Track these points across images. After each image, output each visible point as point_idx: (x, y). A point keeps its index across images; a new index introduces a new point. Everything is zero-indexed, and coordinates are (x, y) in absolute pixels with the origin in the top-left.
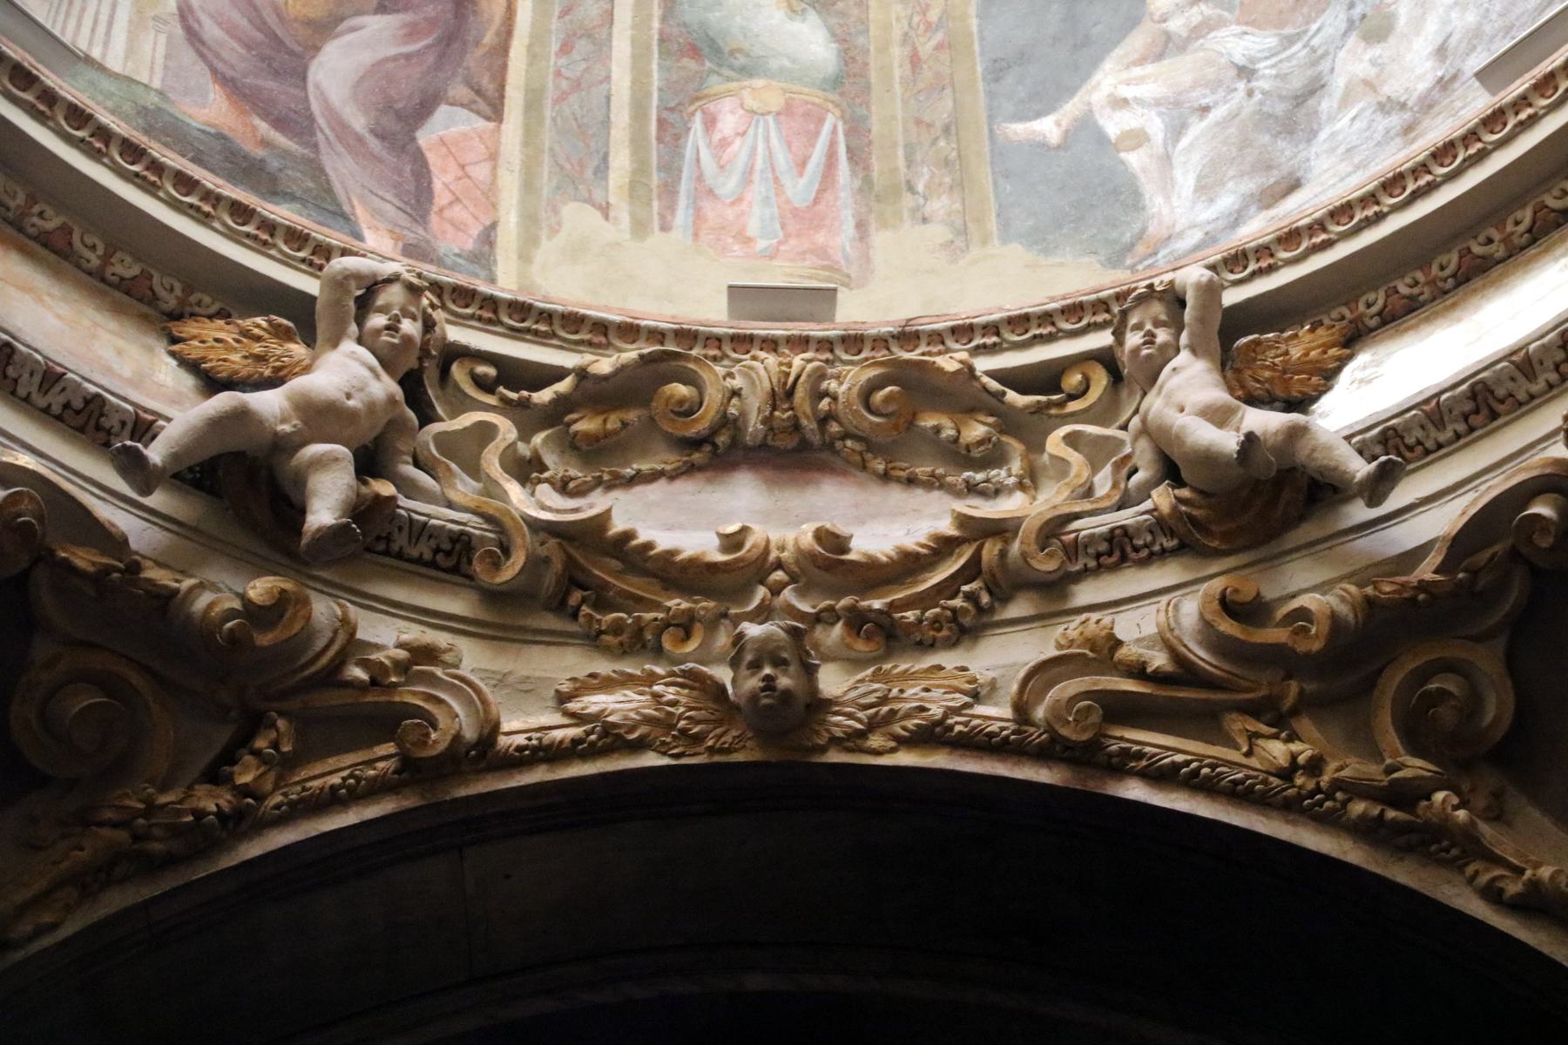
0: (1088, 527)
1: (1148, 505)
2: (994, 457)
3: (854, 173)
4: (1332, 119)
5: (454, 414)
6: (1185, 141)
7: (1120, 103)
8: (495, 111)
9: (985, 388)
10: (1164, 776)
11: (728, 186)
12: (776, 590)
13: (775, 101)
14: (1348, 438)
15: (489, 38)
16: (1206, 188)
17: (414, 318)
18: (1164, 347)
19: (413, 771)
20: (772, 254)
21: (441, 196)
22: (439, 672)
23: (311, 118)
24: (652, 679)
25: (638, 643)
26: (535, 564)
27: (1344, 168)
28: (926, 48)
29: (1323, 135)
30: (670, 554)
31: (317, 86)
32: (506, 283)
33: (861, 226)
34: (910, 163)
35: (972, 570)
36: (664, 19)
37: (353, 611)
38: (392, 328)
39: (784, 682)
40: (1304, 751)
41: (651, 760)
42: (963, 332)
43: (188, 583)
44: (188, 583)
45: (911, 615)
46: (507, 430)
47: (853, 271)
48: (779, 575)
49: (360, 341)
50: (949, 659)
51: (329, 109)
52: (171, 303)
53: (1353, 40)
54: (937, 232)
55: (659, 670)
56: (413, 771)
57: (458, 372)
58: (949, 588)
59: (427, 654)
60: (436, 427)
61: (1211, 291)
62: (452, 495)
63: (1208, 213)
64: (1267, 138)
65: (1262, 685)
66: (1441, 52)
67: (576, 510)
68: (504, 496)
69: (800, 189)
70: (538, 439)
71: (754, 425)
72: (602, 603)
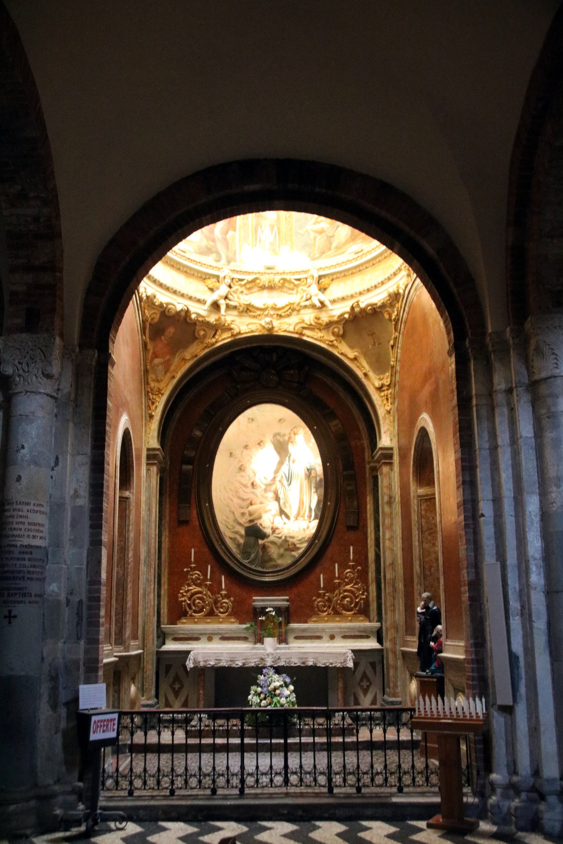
2: (293, 289)
8: (235, 230)
10: (308, 336)
19: (233, 335)
21: (230, 247)
25: (254, 317)
26: (244, 308)
33: (279, 246)
35: (290, 308)
40: (322, 335)
41: (256, 334)
46: (240, 289)
52: (204, 277)
56: (233, 335)
58: (287, 311)
59: (233, 321)
60: (232, 289)
65: (318, 326)
71: (267, 285)
72: (251, 311)
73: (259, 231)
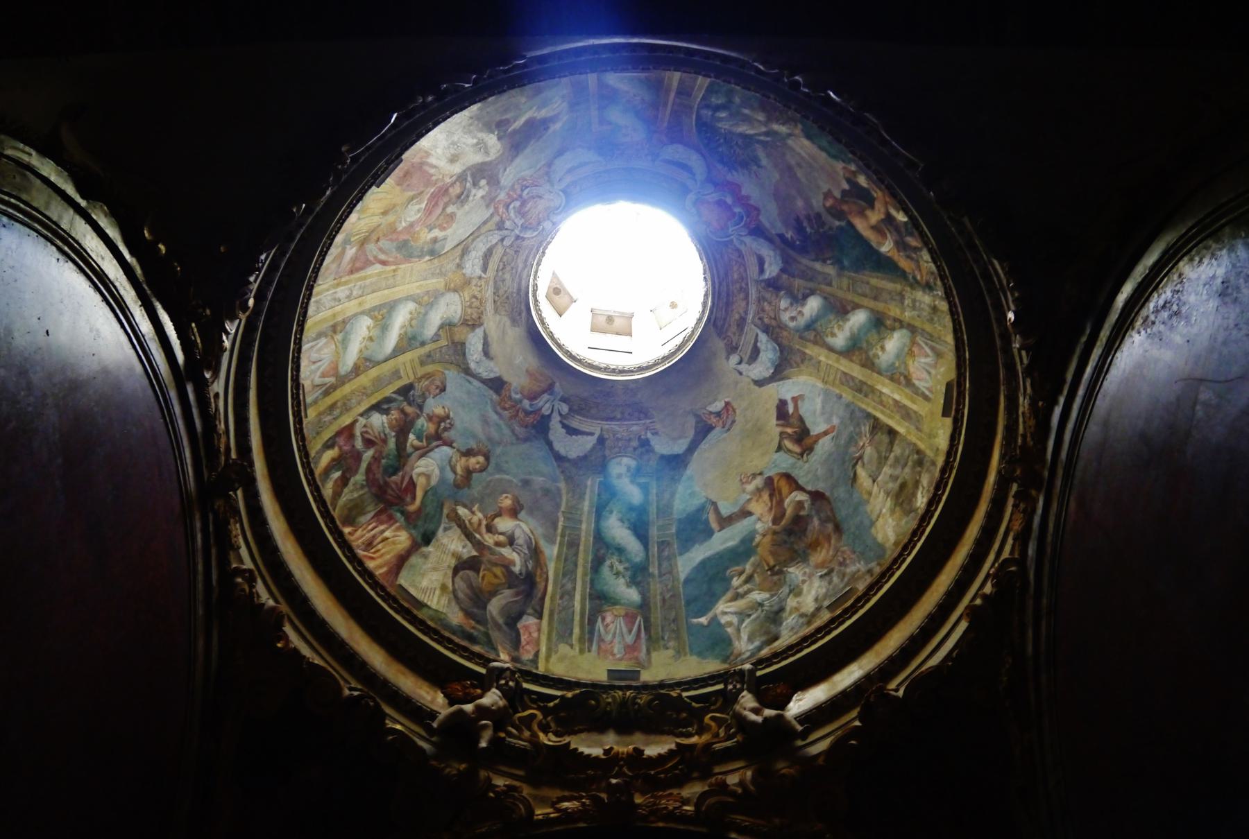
0: (717, 746)
1: (735, 740)
3: (646, 634)
4: (786, 619)
5: (524, 711)
6: (744, 625)
7: (725, 613)
8: (540, 617)
9: (685, 701)
11: (609, 638)
12: (621, 767)
13: (623, 613)
14: (795, 718)
15: (539, 595)
16: (750, 640)
17: (513, 681)
18: (739, 689)
20: (621, 659)
22: (516, 794)
23: (487, 620)
24: (583, 797)
27: (791, 634)
28: (667, 596)
29: (784, 624)
30: (589, 756)
31: (490, 611)
32: (541, 670)
34: (663, 630)
36: (590, 589)
37: (491, 774)
38: (507, 684)
39: (623, 798)
42: (679, 684)
43: (443, 765)
44: (443, 765)
45: (662, 776)
46: (540, 716)
47: (646, 664)
48: (622, 763)
49: (497, 688)
50: (675, 792)
51: (492, 618)
53: (791, 596)
54: (671, 652)
55: (584, 794)
57: (526, 698)
58: (675, 767)
61: (752, 672)
62: (523, 737)
63: (751, 647)
64: (768, 624)
66: (816, 600)
67: (560, 742)
68: (537, 737)
69: (629, 639)
70: (549, 718)
73: (599, 624)
